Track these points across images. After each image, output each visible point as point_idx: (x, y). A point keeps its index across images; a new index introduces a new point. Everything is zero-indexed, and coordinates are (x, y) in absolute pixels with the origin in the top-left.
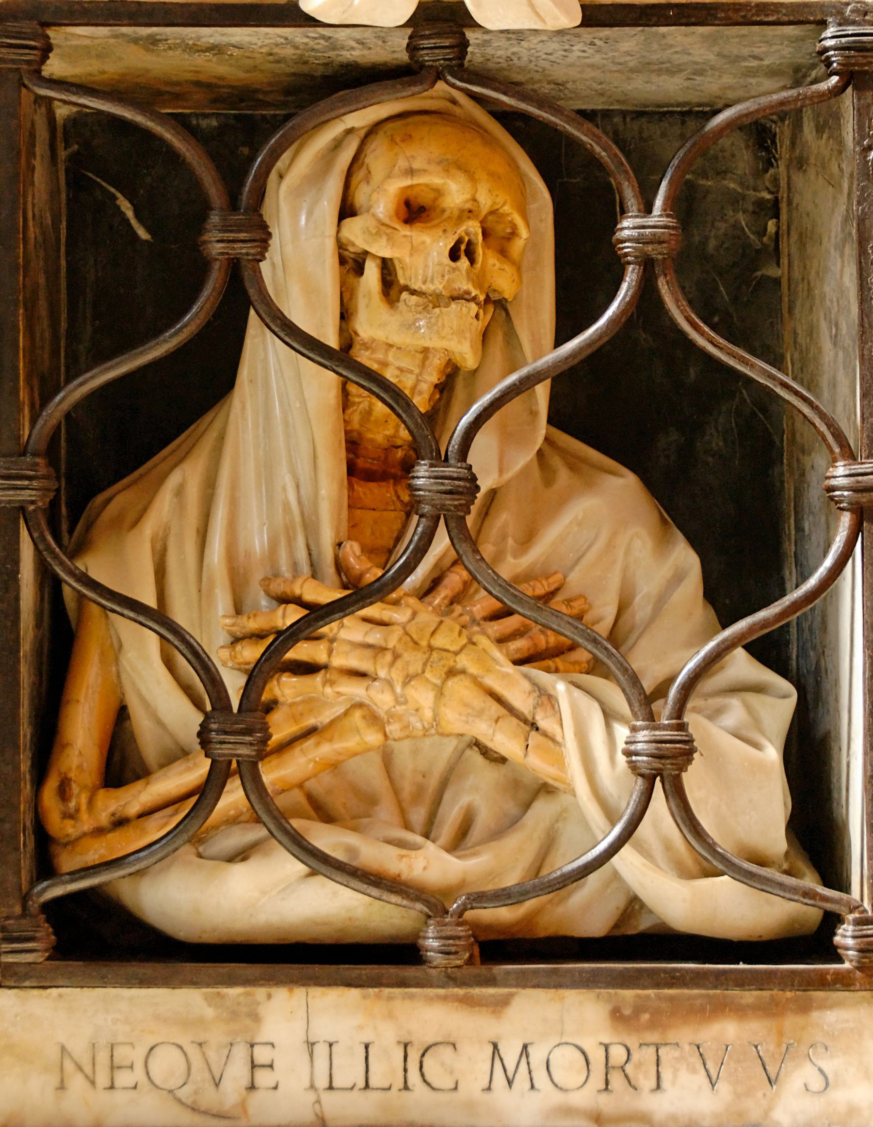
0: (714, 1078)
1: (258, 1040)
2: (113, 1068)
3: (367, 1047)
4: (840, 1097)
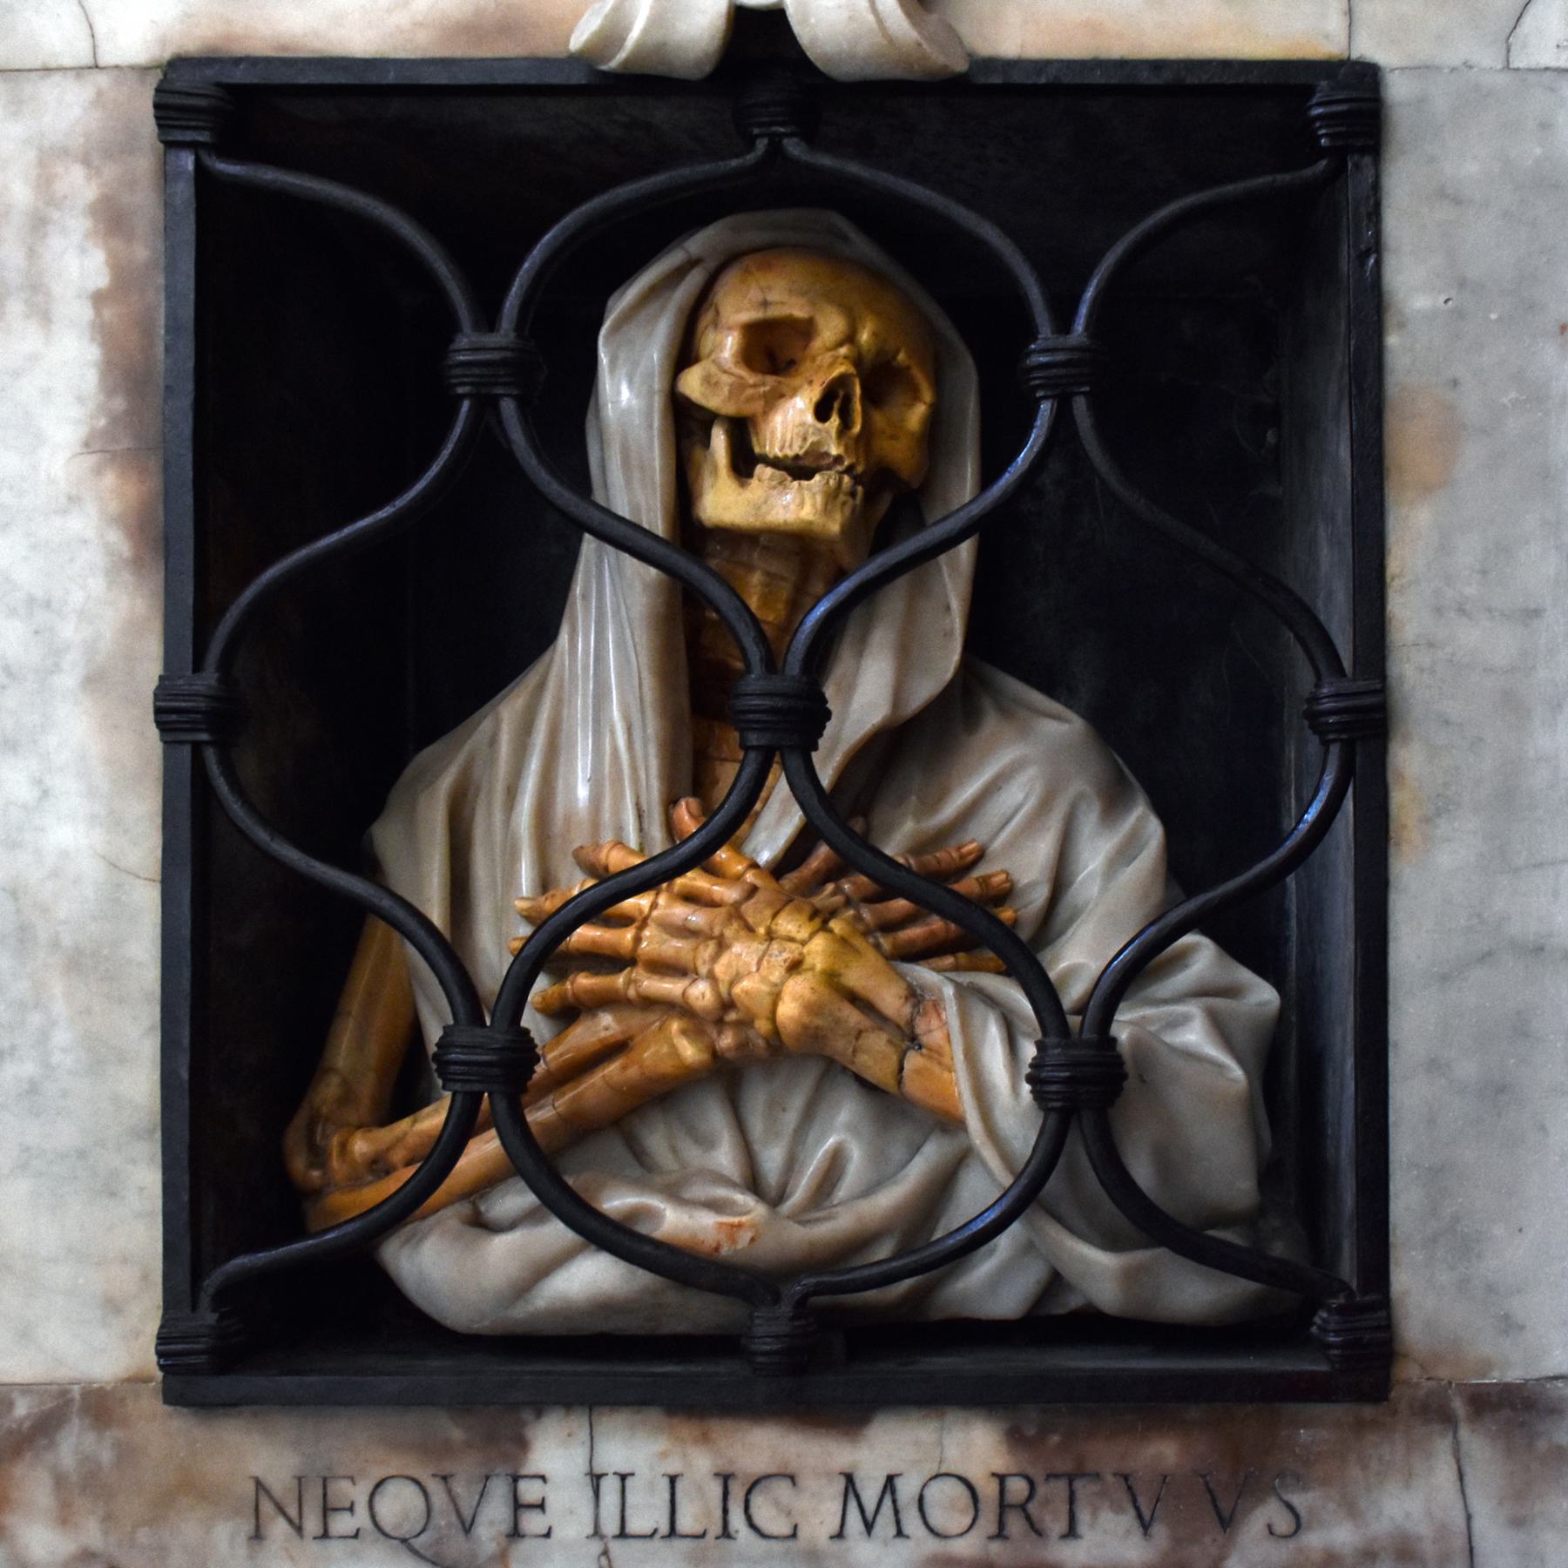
0: (1147, 1517)
1: (524, 1471)
2: (327, 1510)
3: (673, 1480)
4: (1314, 1540)
